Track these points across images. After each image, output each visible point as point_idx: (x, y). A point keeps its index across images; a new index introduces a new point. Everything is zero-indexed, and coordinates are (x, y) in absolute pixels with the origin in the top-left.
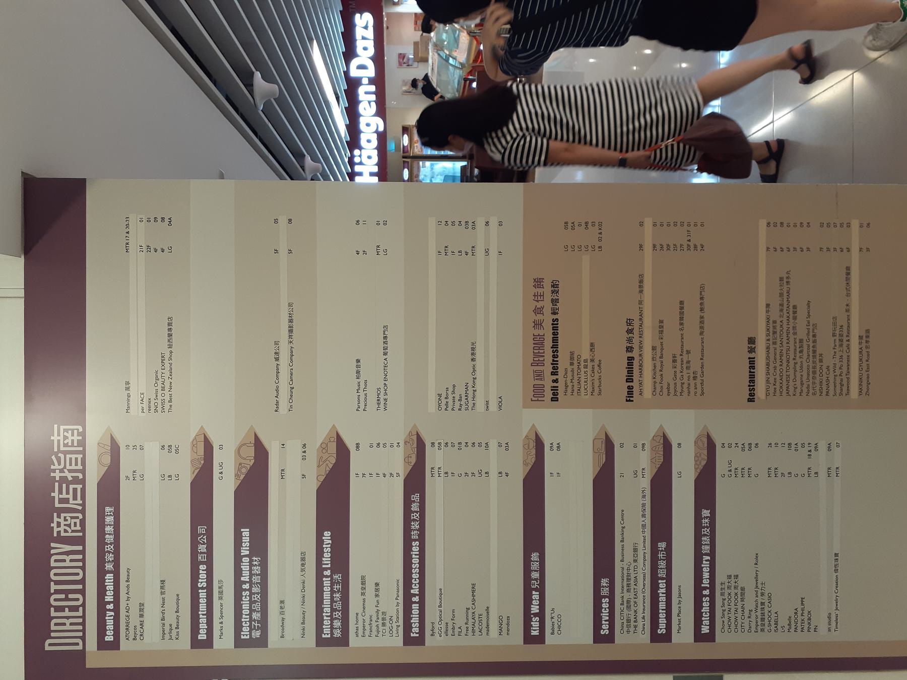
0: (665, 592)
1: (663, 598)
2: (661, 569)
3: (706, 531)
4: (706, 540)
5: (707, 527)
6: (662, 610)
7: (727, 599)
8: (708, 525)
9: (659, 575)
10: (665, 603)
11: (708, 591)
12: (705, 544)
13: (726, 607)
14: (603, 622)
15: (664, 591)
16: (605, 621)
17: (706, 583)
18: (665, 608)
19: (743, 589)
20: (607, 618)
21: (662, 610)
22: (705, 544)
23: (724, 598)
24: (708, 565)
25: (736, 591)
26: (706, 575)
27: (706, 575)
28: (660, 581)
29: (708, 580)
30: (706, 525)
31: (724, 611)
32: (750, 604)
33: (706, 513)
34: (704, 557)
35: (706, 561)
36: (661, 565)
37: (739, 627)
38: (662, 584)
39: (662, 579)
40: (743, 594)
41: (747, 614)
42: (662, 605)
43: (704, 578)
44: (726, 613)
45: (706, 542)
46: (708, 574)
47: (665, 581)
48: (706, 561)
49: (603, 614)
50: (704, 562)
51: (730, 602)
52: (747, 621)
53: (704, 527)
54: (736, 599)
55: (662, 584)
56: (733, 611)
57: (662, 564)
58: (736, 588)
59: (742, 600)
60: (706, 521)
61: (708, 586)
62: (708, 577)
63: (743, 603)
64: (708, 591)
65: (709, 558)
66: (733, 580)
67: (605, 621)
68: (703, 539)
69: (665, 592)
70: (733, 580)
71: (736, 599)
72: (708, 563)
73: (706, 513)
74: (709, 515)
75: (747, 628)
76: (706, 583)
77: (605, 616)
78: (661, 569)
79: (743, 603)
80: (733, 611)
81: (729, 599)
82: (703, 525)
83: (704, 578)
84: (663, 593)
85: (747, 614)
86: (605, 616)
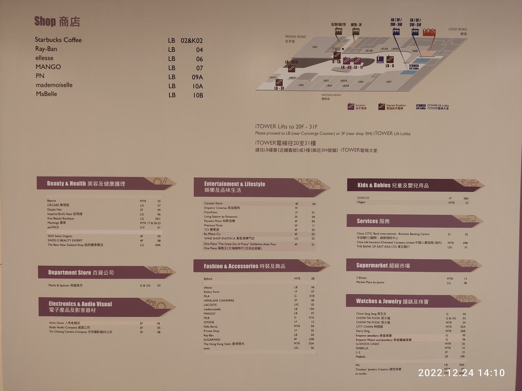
0: (381, 267)
1: (377, 266)
2: (394, 265)
3: (416, 302)
4: (411, 302)
5: (418, 302)
6: (370, 266)
7: (376, 316)
8: (419, 303)
9: (390, 264)
10: (374, 267)
11: (381, 303)
12: (408, 301)
13: (371, 316)
14: (364, 220)
15: (381, 266)
16: (365, 221)
17: (386, 301)
18: (371, 267)
19: (382, 327)
20: (366, 223)
21: (370, 266)
22: (408, 301)
23: (377, 314)
24: (396, 303)
25: (380, 322)
26: (390, 302)
27: (390, 302)
28: (387, 264)
29: (387, 303)
30: (419, 302)
31: (369, 314)
32: (374, 331)
33: (426, 302)
34: (401, 300)
35: (399, 302)
36: (397, 265)
37: (360, 324)
38: (385, 266)
39: (388, 266)
40: (378, 326)
41: (367, 329)
42: (373, 266)
43: (388, 300)
44: (368, 316)
45: (409, 302)
46: (391, 303)
47: (387, 267)
48: (399, 302)
49: (369, 220)
50: (398, 301)
51: (374, 318)
52: (363, 329)
53: (418, 301)
54: (376, 322)
55: (385, 266)
56: (369, 320)
57: (397, 266)
58: (383, 322)
59: (375, 326)
60: (422, 302)
61: (384, 303)
62: (389, 303)
63: (373, 327)
64: (381, 303)
65: (400, 303)
66: (387, 320)
67: (365, 221)
68: (411, 300)
69: (381, 267)
70: (387, 320)
71: (376, 322)
72: (397, 303)
73: (426, 302)
74: (425, 304)
75: (359, 329)
76: (386, 301)
77: (368, 221)
78: (394, 265)
79: (373, 327)
80: (369, 320)
81: (376, 318)
82: (419, 300)
83: (388, 300)
84: (380, 266)
85: (367, 329)
86: (368, 221)
